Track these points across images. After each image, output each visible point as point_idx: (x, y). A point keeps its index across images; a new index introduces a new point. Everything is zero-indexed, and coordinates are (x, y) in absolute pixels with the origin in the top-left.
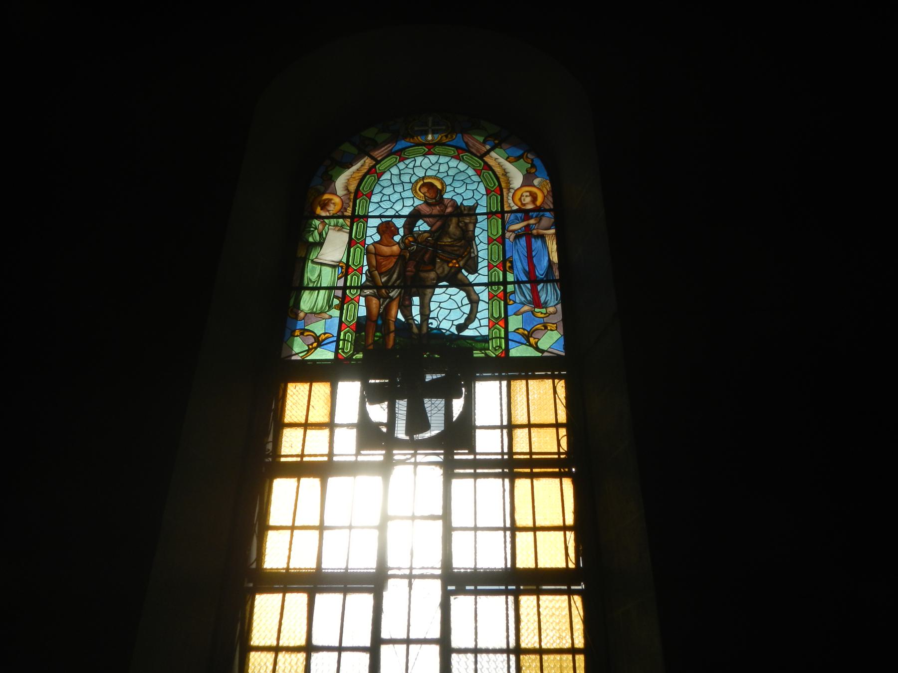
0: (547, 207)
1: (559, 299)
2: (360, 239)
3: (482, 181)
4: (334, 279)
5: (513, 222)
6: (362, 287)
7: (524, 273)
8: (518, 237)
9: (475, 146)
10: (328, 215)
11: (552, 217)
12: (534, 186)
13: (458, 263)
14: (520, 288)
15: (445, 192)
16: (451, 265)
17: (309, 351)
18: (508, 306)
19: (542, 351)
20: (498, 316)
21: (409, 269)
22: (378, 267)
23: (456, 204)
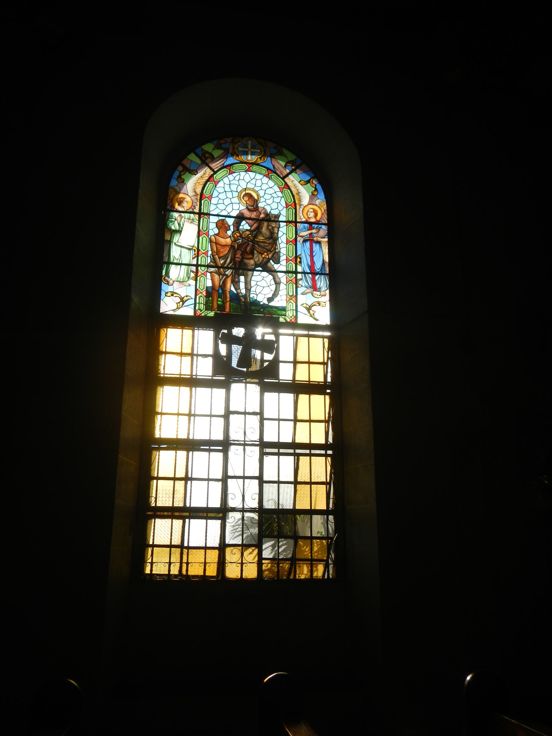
0: (324, 222)
1: (328, 286)
2: (205, 231)
4: (190, 259)
5: (302, 230)
6: (208, 266)
7: (308, 266)
8: (305, 241)
10: (183, 210)
12: (316, 205)
13: (268, 255)
14: (305, 277)
16: (263, 256)
18: (298, 288)
21: (237, 256)
22: (218, 252)
23: (266, 212)
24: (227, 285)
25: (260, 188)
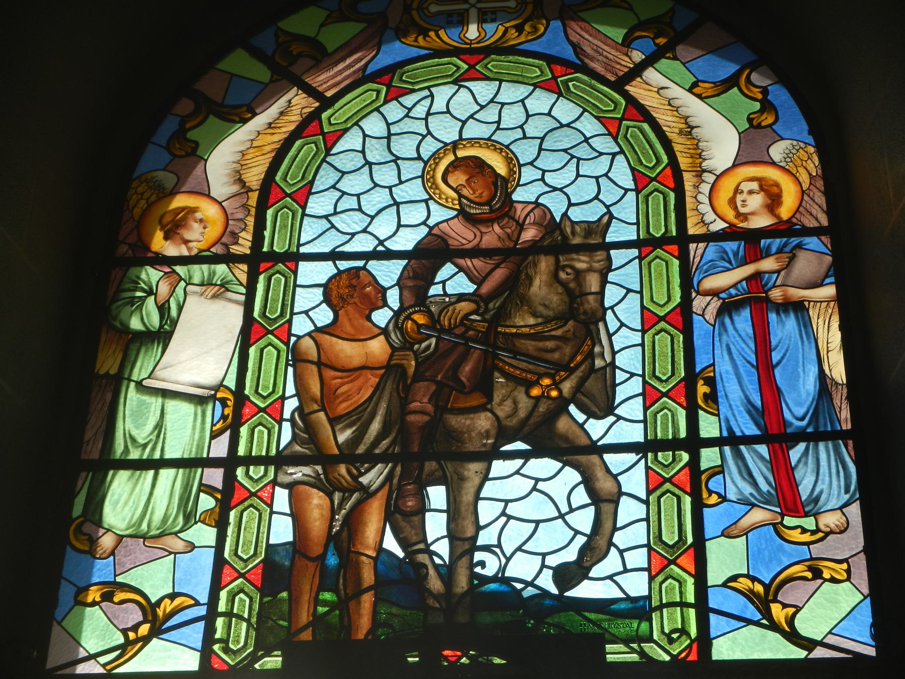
0: (811, 223)
1: (853, 488)
2: (275, 320)
3: (622, 152)
4: (202, 438)
6: (281, 460)
7: (749, 413)
8: (728, 308)
9: (601, 54)
10: (185, 253)
11: (828, 252)
12: (773, 164)
13: (556, 385)
14: (739, 456)
15: (518, 185)
16: (535, 392)
17: (125, 649)
18: (705, 510)
19: (809, 644)
20: (676, 539)
21: (415, 405)
22: (327, 400)
23: (549, 216)
24: (363, 532)
25: (519, 134)
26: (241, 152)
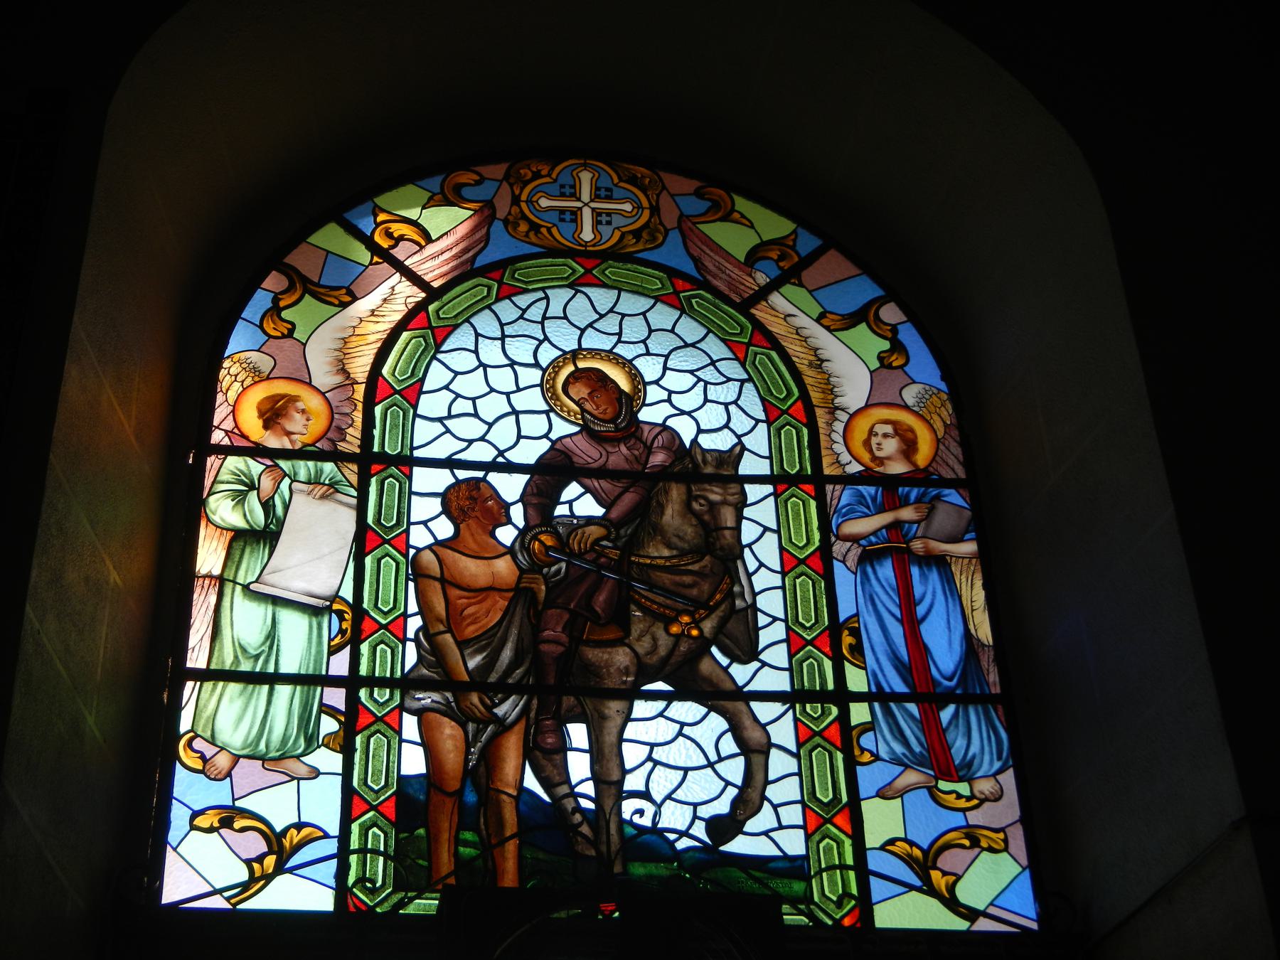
0: (948, 474)
1: (1005, 754)
3: (750, 379)
4: (319, 652)
5: (853, 511)
6: (407, 684)
9: (724, 272)
10: (289, 446)
11: (966, 506)
12: (906, 407)
13: (696, 623)
14: (888, 713)
15: (644, 404)
16: (675, 629)
17: (256, 880)
18: (859, 768)
19: (971, 914)
20: (831, 796)
22: (453, 621)
23: (677, 442)
24: (502, 769)
25: (640, 349)
26: (343, 339)
